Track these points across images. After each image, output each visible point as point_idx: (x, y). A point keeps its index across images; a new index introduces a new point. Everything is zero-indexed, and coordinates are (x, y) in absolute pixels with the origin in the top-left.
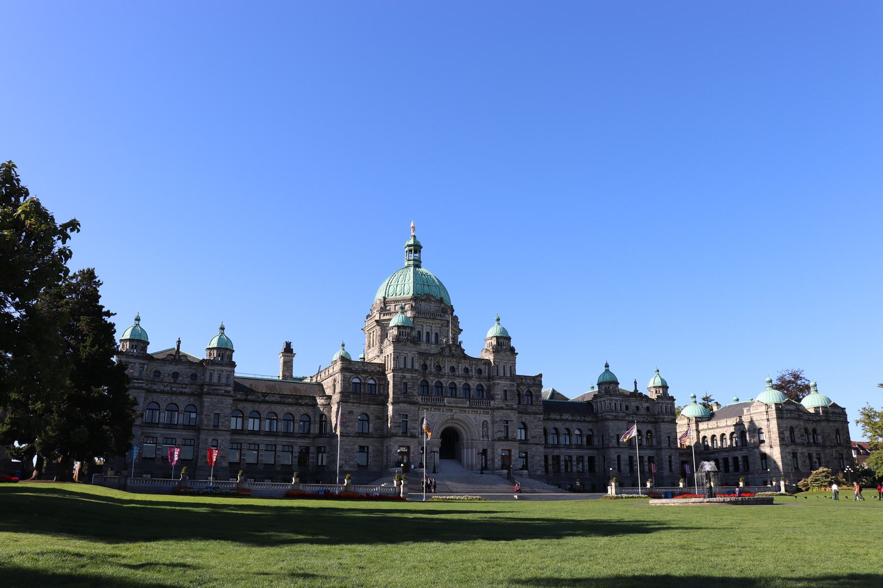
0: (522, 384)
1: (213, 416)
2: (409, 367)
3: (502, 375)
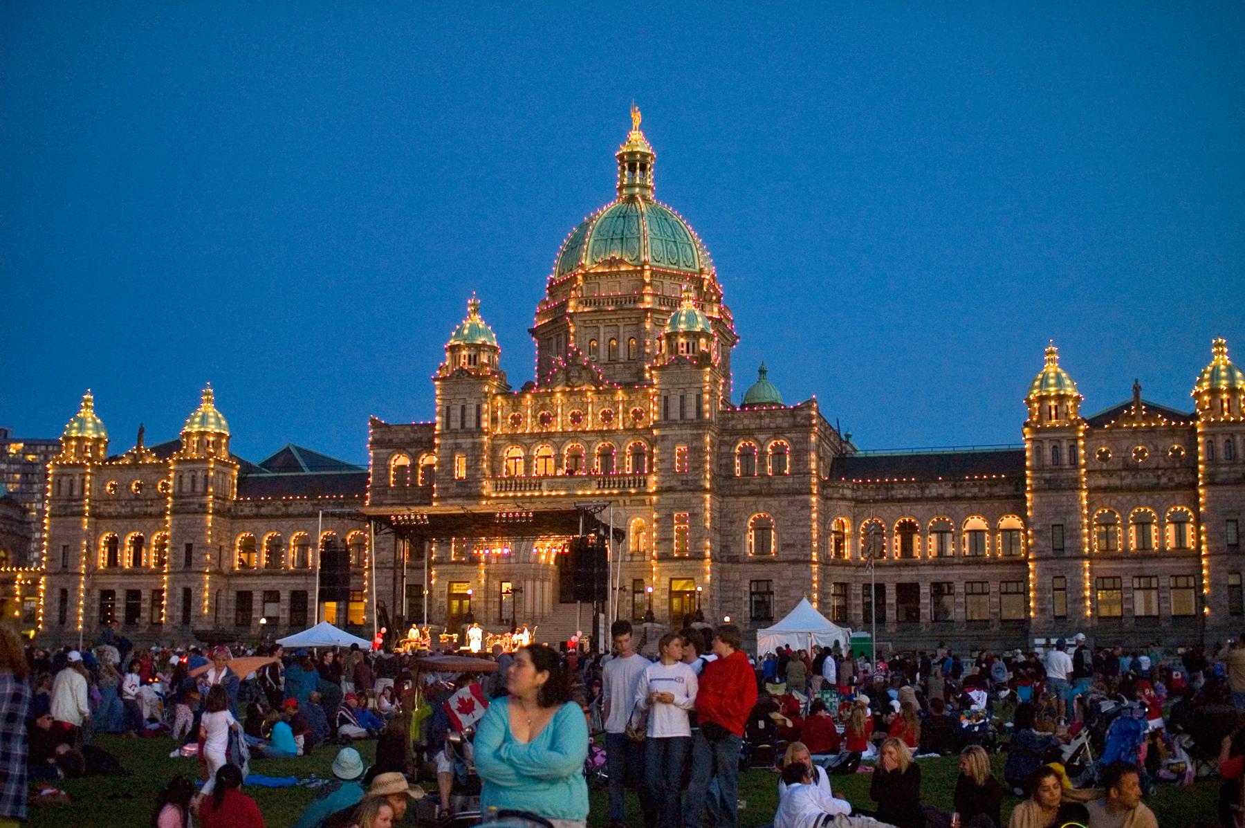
0: (761, 429)
1: (183, 550)
2: (471, 424)
3: (675, 414)
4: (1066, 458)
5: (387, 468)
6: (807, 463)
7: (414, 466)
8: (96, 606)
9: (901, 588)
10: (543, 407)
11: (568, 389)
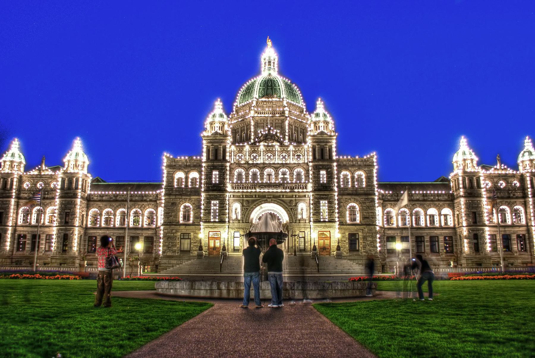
4: (475, 184)
5: (173, 178)
6: (372, 182)
7: (187, 178)
8: (16, 242)
9: (431, 237)
10: (254, 151)
11: (266, 144)
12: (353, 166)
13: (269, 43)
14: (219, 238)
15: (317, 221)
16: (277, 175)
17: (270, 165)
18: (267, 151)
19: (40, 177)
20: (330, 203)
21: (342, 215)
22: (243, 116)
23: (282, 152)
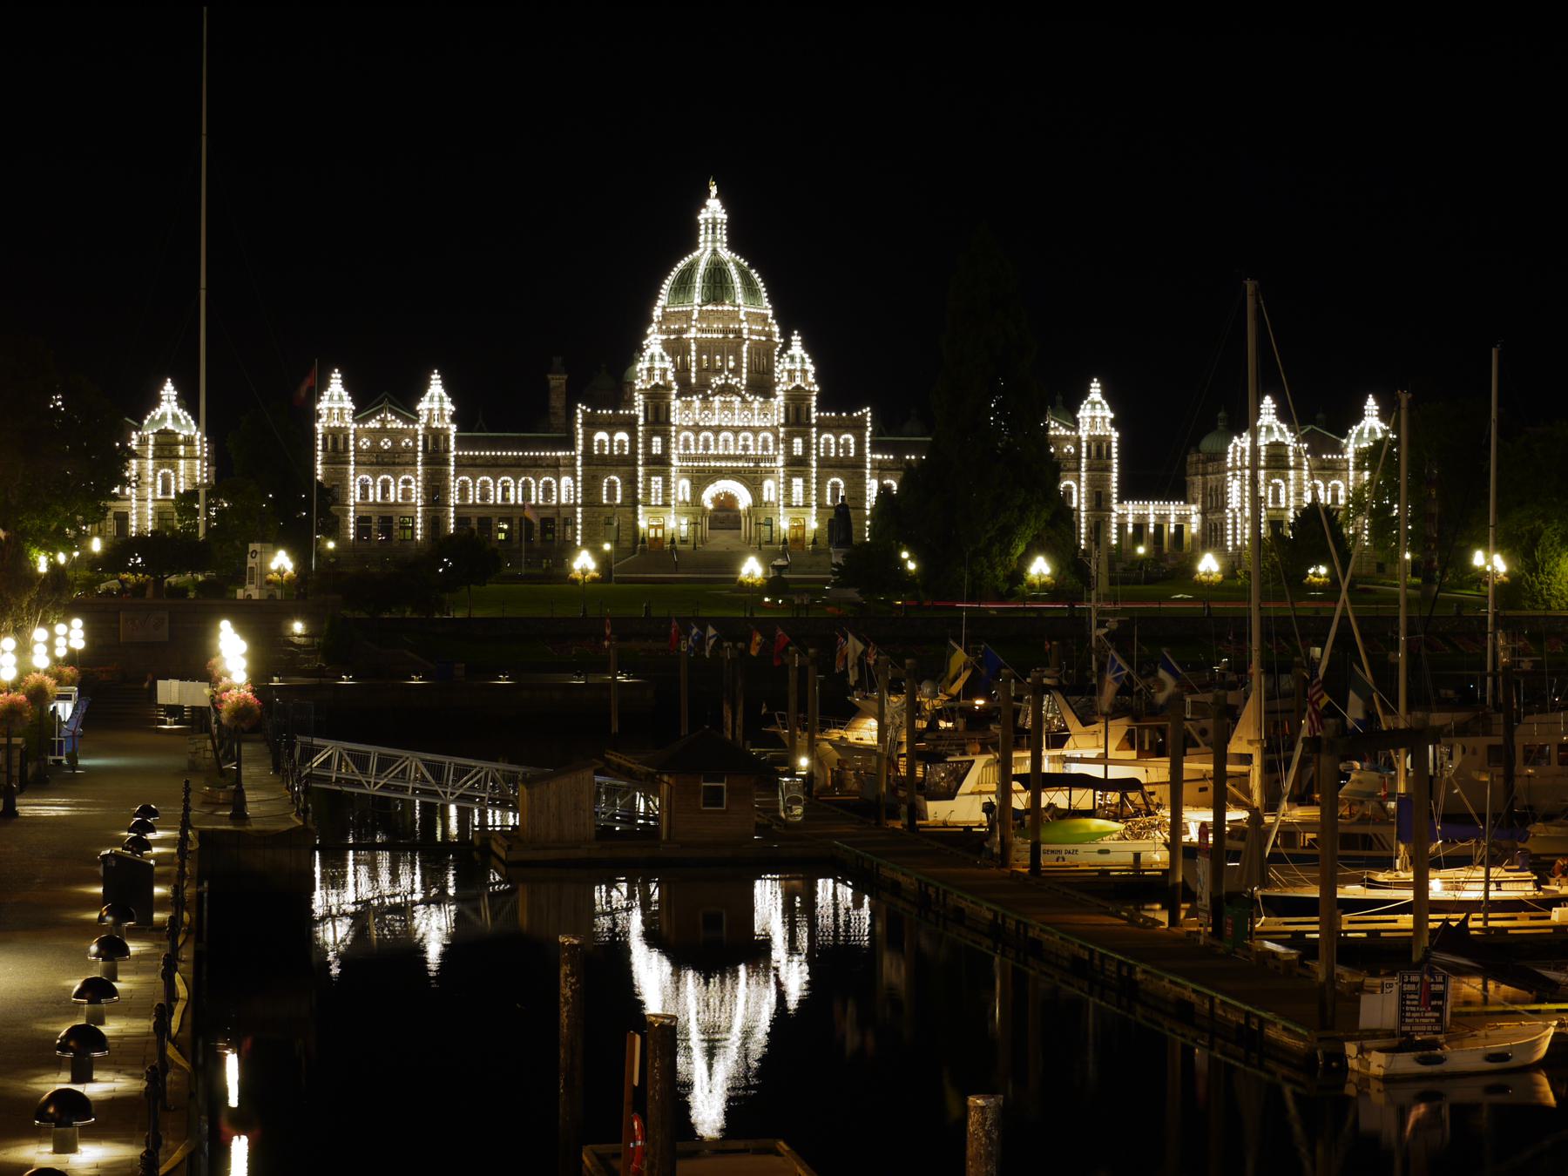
7: (611, 441)
10: (706, 408)
12: (839, 427)
13: (714, 190)
14: (662, 527)
15: (788, 505)
16: (736, 441)
17: (727, 428)
18: (723, 409)
19: (383, 431)
20: (807, 481)
21: (821, 493)
22: (681, 331)
23: (743, 409)
